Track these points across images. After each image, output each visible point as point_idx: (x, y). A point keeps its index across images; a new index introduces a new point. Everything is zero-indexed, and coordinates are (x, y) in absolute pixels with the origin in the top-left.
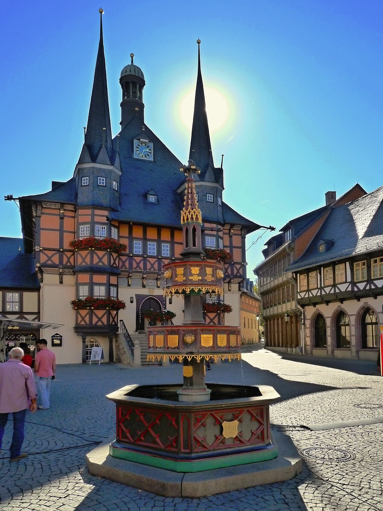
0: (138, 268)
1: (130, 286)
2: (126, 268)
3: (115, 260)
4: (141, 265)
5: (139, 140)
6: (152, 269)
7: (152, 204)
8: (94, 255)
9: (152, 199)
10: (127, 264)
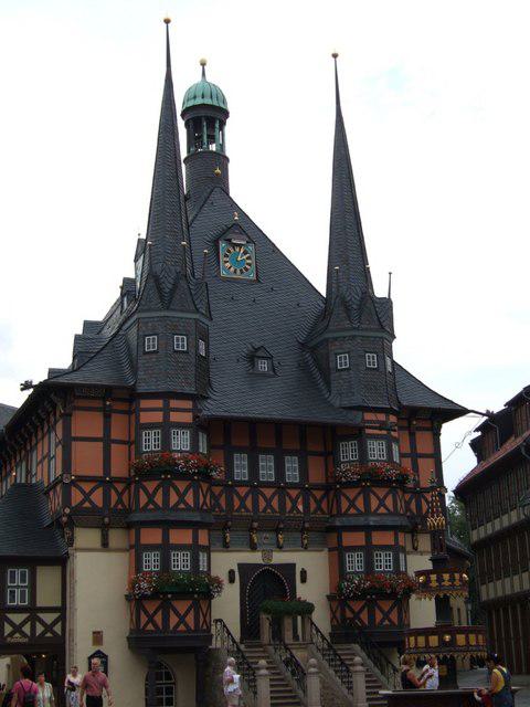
3: (205, 497)
4: (249, 503)
5: (229, 240)
7: (264, 375)
8: (171, 489)
9: (263, 366)
10: (222, 501)
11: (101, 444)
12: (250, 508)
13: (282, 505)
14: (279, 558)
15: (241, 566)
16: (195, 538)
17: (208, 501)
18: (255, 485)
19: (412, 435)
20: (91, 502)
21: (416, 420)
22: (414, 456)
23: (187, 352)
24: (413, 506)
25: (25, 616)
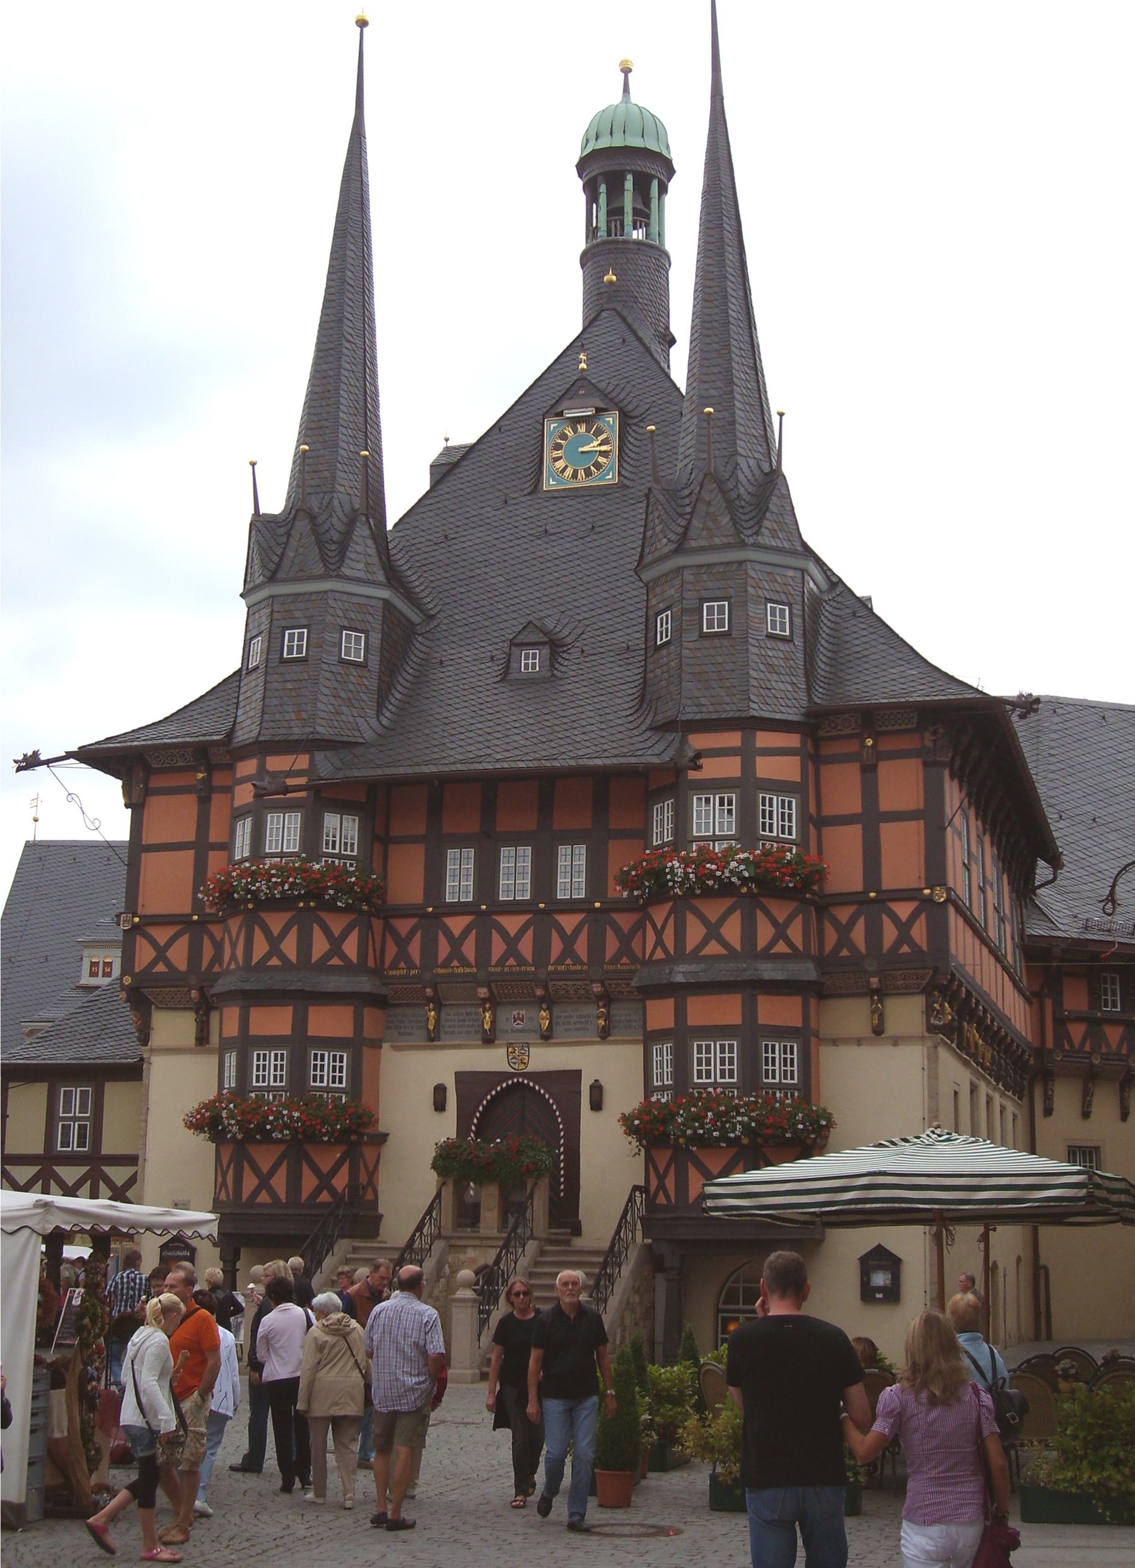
0: (455, 963)
1: (432, 1040)
2: (411, 966)
4: (469, 949)
5: (561, 414)
6: (511, 961)
7: (530, 682)
9: (531, 662)
10: (415, 950)
11: (192, 852)
12: (472, 960)
13: (542, 947)
14: (545, 1058)
15: (460, 1077)
16: (300, 1023)
17: (350, 947)
18: (487, 907)
19: (869, 770)
20: (168, 963)
21: (876, 736)
22: (871, 818)
23: (303, 660)
24: (858, 934)
25: (83, 1170)
